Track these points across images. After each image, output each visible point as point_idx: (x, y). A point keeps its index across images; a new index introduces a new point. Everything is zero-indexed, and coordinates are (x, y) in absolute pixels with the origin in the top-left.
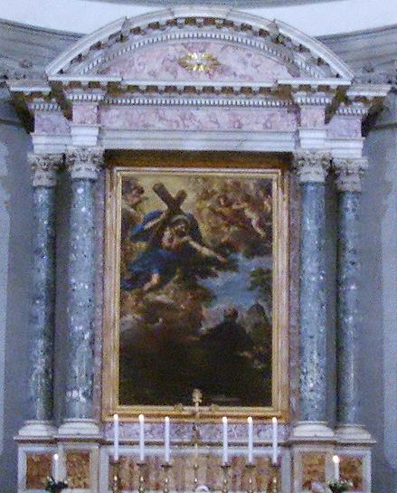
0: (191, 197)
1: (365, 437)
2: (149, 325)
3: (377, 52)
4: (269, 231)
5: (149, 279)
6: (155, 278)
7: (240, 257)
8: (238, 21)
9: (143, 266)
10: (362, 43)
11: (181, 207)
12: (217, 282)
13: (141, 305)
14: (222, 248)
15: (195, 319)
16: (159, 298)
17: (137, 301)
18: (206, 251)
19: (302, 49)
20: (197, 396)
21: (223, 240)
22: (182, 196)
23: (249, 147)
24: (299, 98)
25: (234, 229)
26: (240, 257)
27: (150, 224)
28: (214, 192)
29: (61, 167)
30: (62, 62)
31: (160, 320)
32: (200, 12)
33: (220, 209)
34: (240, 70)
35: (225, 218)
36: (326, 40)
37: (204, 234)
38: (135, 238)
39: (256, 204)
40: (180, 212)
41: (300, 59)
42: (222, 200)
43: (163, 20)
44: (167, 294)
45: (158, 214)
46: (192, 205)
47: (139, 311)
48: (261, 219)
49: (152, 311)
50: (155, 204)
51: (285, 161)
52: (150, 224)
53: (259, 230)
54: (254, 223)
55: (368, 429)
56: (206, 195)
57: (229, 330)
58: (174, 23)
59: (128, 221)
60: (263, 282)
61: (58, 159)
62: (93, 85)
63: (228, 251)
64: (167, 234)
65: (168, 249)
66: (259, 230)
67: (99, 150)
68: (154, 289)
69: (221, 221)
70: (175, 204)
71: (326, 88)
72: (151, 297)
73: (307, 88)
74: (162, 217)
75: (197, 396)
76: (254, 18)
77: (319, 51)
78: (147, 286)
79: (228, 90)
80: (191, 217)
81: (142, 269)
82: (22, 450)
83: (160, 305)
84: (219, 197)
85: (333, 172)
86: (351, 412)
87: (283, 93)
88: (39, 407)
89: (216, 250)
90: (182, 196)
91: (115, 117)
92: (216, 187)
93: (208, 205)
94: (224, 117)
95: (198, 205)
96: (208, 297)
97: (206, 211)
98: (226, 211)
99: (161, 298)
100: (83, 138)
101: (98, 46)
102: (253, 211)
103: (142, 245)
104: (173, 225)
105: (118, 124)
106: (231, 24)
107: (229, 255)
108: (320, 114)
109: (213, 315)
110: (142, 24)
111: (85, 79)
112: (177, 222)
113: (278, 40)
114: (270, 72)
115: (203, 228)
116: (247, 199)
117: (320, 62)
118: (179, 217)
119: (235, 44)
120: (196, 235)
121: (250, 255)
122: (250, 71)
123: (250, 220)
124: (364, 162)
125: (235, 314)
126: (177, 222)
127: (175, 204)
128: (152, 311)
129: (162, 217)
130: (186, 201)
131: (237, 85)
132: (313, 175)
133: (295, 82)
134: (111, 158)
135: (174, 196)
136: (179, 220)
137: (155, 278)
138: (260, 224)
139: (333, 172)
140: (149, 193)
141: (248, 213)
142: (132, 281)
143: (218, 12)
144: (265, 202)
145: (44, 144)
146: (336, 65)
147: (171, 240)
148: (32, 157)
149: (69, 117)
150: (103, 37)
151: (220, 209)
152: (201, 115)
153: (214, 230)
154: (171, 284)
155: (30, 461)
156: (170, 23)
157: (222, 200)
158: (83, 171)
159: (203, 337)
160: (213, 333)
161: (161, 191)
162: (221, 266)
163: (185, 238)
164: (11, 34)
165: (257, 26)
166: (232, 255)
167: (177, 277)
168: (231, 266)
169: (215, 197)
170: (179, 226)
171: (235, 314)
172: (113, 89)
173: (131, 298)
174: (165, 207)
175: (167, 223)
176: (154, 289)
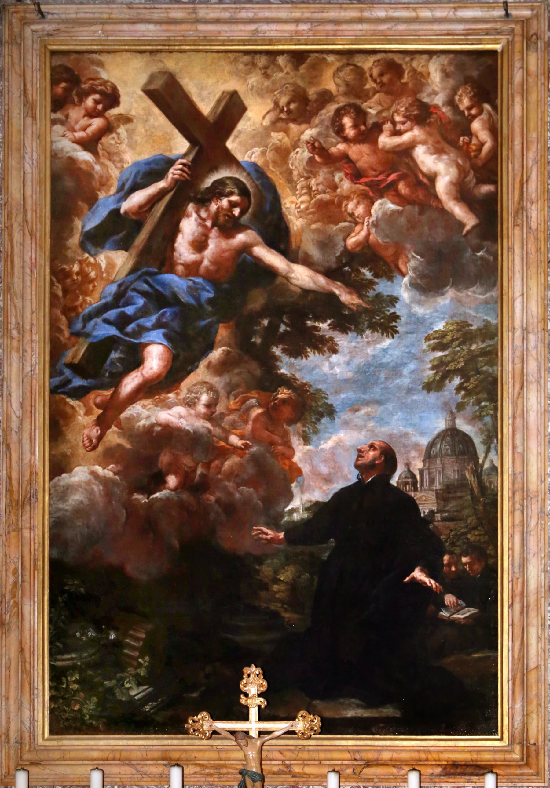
2: (141, 498)
5: (135, 360)
6: (155, 358)
7: (402, 290)
9: (122, 322)
11: (230, 144)
13: (113, 437)
16: (165, 416)
17: (103, 423)
18: (302, 276)
21: (351, 241)
25: (384, 206)
26: (402, 290)
27: (138, 198)
28: (326, 98)
31: (172, 481)
33: (342, 147)
35: (356, 175)
37: (296, 223)
40: (230, 160)
42: (347, 121)
44: (190, 404)
46: (261, 137)
47: (111, 455)
48: (462, 172)
52: (138, 198)
53: (458, 211)
54: (442, 186)
56: (302, 108)
63: (367, 273)
64: (189, 226)
65: (192, 269)
66: (458, 211)
68: (151, 389)
69: (346, 185)
74: (174, 173)
78: (130, 383)
80: (258, 172)
81: (113, 331)
83: (168, 435)
84: (339, 114)
89: (330, 274)
90: (232, 108)
92: (330, 83)
93: (309, 133)
95: (276, 137)
97: (302, 154)
98: (360, 153)
99: (174, 414)
102: (438, 151)
104: (203, 201)
107: (371, 284)
112: (218, 190)
115: (294, 206)
118: (223, 173)
120: (277, 235)
121: (429, 285)
123: (432, 178)
126: (218, 190)
129: (174, 173)
130: (241, 125)
135: (206, 107)
136: (221, 182)
137: (155, 358)
140: (133, 101)
141: (426, 159)
144: (476, 125)
147: (199, 245)
151: (342, 147)
153: (328, 211)
154: (201, 373)
157: (347, 121)
163: (241, 238)
166: (383, 287)
167: (216, 354)
169: (332, 108)
170: (225, 202)
174: (181, 145)
176: (151, 389)
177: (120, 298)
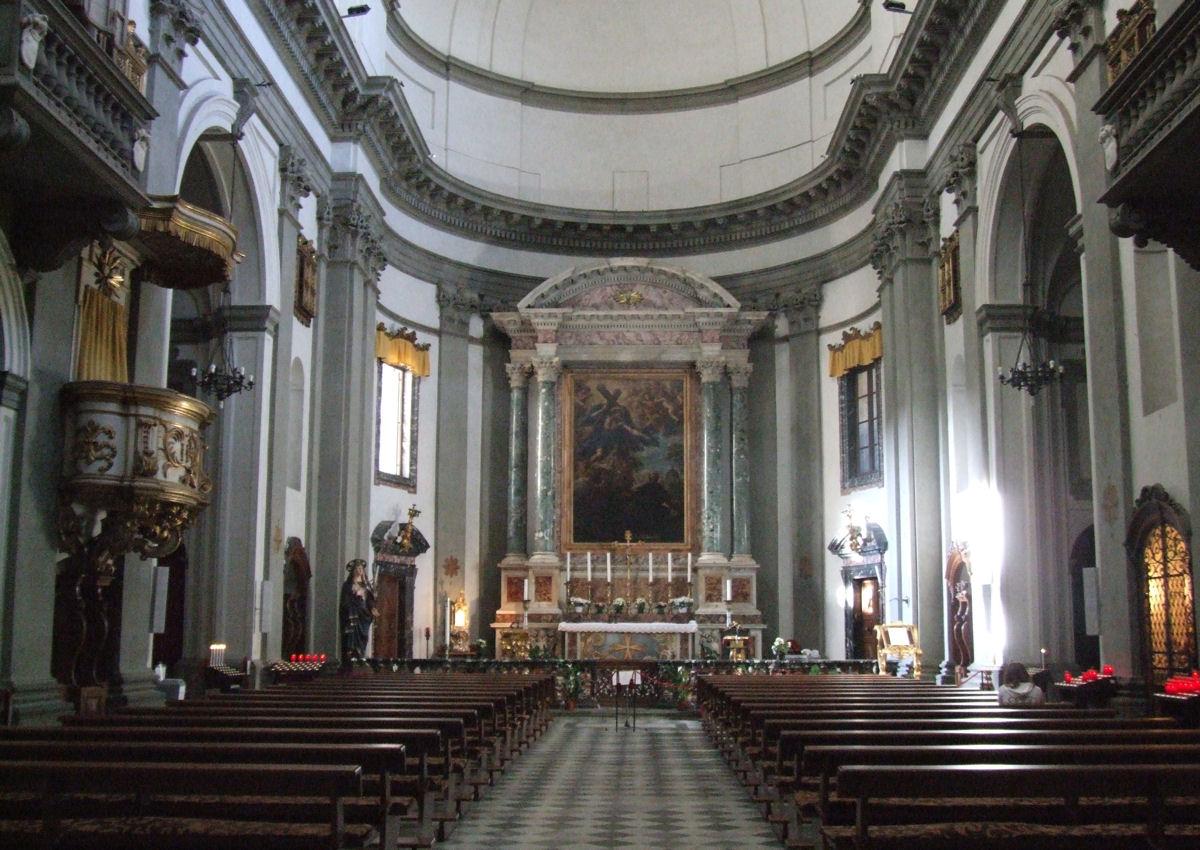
0: (624, 394)
1: (753, 563)
6: (599, 452)
10: (746, 281)
12: (645, 453)
15: (628, 479)
18: (635, 432)
20: (628, 535)
22: (618, 393)
23: (666, 357)
45: (600, 406)
49: (597, 476)
59: (579, 412)
60: (677, 453)
70: (612, 399)
72: (597, 465)
75: (628, 535)
82: (504, 575)
85: (726, 373)
90: (618, 393)
103: (589, 429)
106: (652, 270)
113: (686, 282)
116: (665, 394)
120: (629, 422)
121: (667, 435)
124: (750, 367)
125: (657, 476)
128: (597, 476)
137: (599, 452)
142: (582, 454)
146: (729, 298)
162: (647, 444)
171: (657, 476)
173: (582, 465)
175: (606, 412)
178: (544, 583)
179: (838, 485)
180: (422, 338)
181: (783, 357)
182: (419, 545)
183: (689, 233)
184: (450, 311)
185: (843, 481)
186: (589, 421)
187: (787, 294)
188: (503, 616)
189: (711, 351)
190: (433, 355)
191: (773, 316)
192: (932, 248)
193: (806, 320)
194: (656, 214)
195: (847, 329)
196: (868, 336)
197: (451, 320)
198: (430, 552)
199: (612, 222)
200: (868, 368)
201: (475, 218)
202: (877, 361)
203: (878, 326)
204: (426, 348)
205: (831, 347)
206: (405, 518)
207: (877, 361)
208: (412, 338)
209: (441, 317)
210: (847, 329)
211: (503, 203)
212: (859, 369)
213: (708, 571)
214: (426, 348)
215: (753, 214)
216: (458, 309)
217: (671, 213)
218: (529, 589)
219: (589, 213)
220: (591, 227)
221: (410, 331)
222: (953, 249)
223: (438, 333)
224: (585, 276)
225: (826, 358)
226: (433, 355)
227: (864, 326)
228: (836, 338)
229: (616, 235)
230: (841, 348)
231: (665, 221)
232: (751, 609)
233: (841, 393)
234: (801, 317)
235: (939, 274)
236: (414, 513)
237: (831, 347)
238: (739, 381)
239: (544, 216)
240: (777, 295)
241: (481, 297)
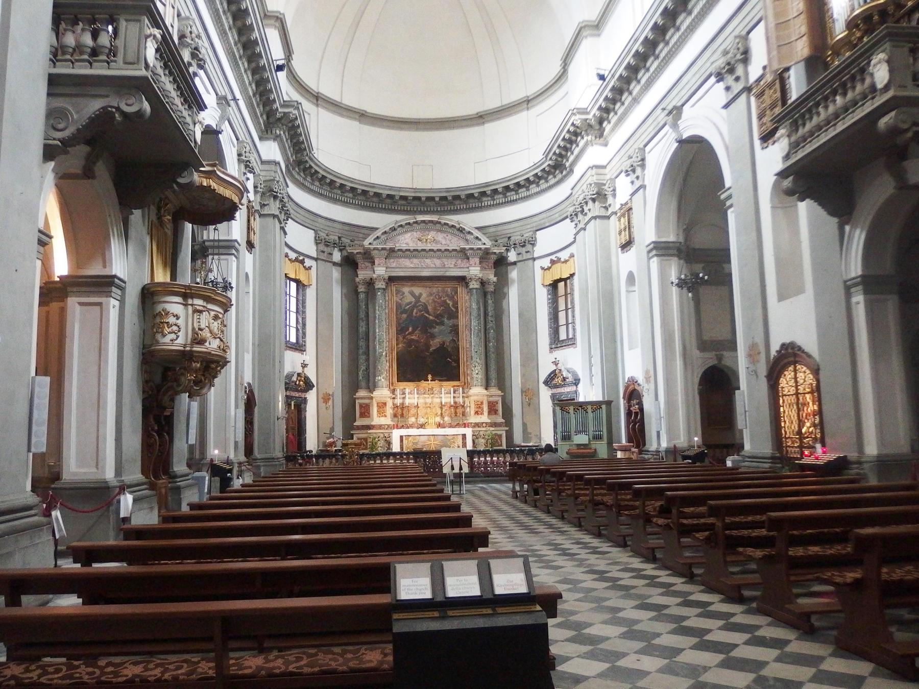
0: (424, 295)
1: (499, 393)
3: (499, 233)
4: (457, 308)
6: (410, 329)
8: (443, 221)
10: (492, 230)
12: (436, 330)
14: (437, 316)
15: (428, 346)
18: (431, 318)
19: (469, 233)
20: (430, 377)
22: (421, 294)
23: (448, 274)
24: (469, 253)
29: (370, 283)
30: (370, 239)
32: (427, 218)
34: (444, 242)
36: (479, 229)
38: (402, 313)
39: (452, 298)
41: (469, 237)
43: (411, 221)
45: (410, 303)
49: (410, 343)
50: (409, 299)
51: (462, 280)
55: (500, 389)
57: (442, 348)
58: (416, 222)
59: (399, 306)
60: (455, 330)
61: (368, 280)
62: (383, 249)
67: (386, 276)
70: (418, 298)
71: (480, 249)
72: (409, 337)
73: (472, 249)
75: (430, 377)
76: (451, 220)
77: (477, 233)
79: (439, 250)
82: (357, 401)
85: (483, 283)
86: (493, 382)
87: (463, 251)
88: (363, 384)
90: (421, 294)
91: (393, 263)
94: (438, 262)
96: (433, 336)
100: (380, 271)
101: (385, 233)
103: (405, 316)
105: (394, 265)
106: (440, 223)
108: (477, 260)
109: (435, 344)
110: (403, 223)
111: (380, 247)
113: (461, 230)
114: (455, 243)
115: (430, 308)
116: (447, 295)
117: (477, 238)
119: (441, 231)
120: (428, 312)
121: (449, 319)
122: (448, 242)
124: (495, 279)
125: (444, 343)
127: (418, 298)
128: (410, 343)
131: (443, 248)
132: (474, 285)
133: (467, 247)
134: (392, 280)
137: (410, 329)
138: (453, 306)
139: (483, 283)
140: (407, 294)
142: (401, 330)
143: (434, 218)
145: (363, 274)
146: (484, 239)
148: (357, 280)
149: (373, 263)
150: (387, 229)
152: (428, 261)
153: (435, 309)
155: (361, 406)
156: (414, 223)
158: (380, 285)
159: (431, 354)
160: (437, 351)
161: (412, 294)
162: (437, 324)
164: (346, 228)
165: (451, 223)
168: (442, 324)
171: (444, 343)
172: (392, 250)
173: (401, 338)
175: (414, 306)
177: (406, 320)
178: (382, 406)
179: (548, 347)
180: (308, 262)
181: (514, 274)
182: (309, 385)
183: (457, 202)
184: (322, 247)
185: (551, 344)
186: (405, 312)
187: (516, 238)
188: (358, 426)
189: (474, 270)
190: (314, 270)
191: (508, 250)
192: (610, 210)
193: (527, 252)
194: (440, 190)
195: (553, 257)
196: (566, 261)
197: (323, 252)
198: (315, 389)
199: (413, 195)
200: (565, 280)
201: (335, 191)
202: (572, 275)
203: (572, 256)
204: (310, 268)
205: (542, 268)
206: (300, 370)
207: (572, 275)
208: (302, 262)
209: (317, 250)
210: (553, 257)
211: (352, 182)
212: (560, 280)
213: (476, 398)
214: (310, 268)
215: (495, 191)
216: (327, 246)
217: (448, 190)
218: (374, 410)
219: (400, 189)
220: (402, 198)
221: (301, 258)
222: (627, 211)
223: (316, 259)
224: (401, 226)
225: (538, 273)
226: (314, 270)
227: (564, 255)
228: (546, 263)
229: (415, 203)
230: (549, 268)
231: (444, 194)
232: (500, 420)
233: (549, 294)
234: (524, 250)
235: (614, 224)
236: (304, 366)
237: (542, 268)
238: (491, 288)
239: (375, 190)
240: (509, 238)
241: (339, 238)
